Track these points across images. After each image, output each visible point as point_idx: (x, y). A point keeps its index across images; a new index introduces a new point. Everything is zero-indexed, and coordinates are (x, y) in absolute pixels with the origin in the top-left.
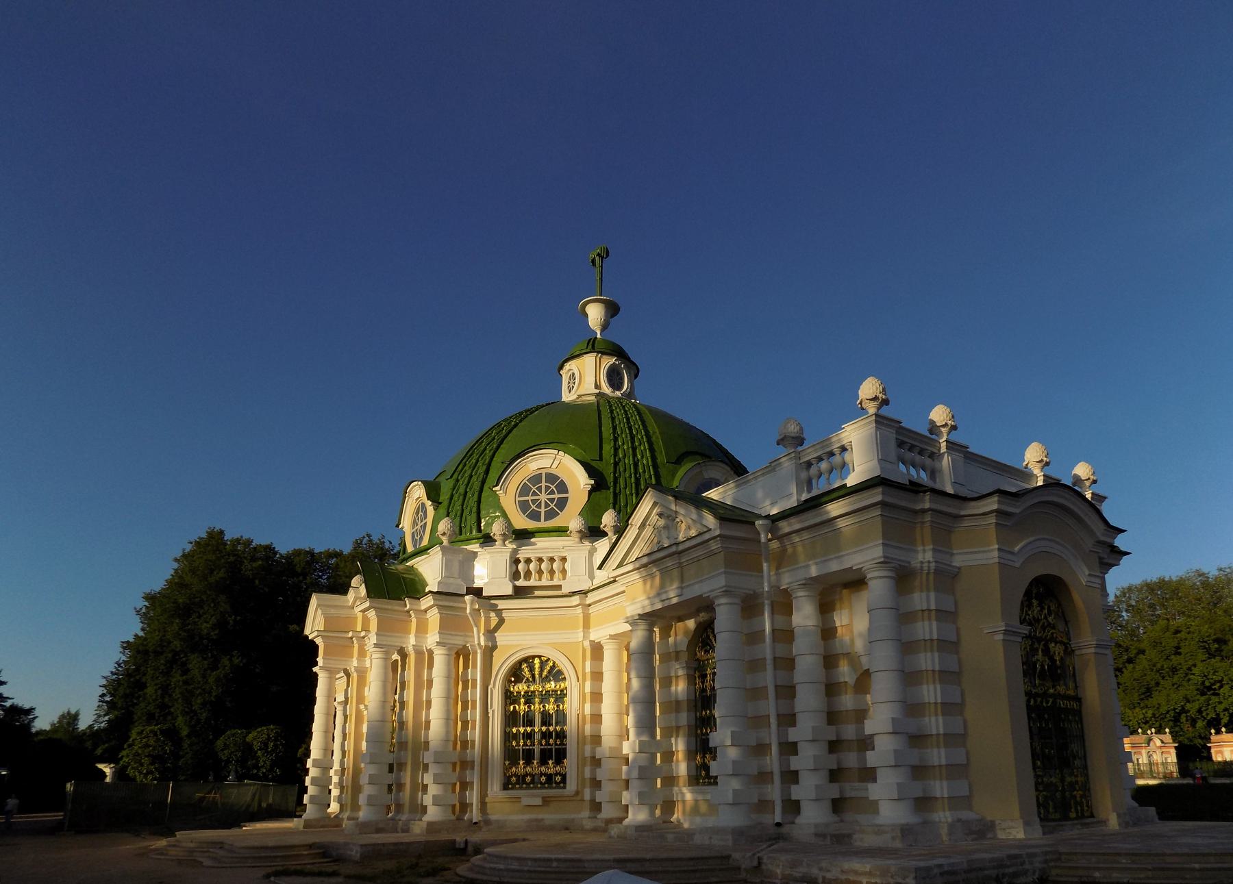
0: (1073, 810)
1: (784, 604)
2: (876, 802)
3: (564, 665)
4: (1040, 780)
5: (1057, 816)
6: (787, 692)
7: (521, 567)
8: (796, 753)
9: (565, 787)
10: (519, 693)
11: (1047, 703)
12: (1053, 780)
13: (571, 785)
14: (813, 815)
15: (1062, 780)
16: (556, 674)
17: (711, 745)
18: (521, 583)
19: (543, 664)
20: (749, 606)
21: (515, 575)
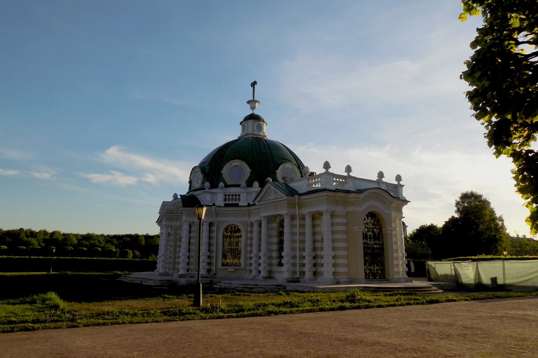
0: (378, 276)
1: (303, 218)
2: (323, 272)
3: (241, 227)
4: (367, 267)
5: (372, 278)
6: (303, 241)
7: (227, 197)
8: (305, 259)
9: (240, 266)
10: (228, 236)
11: (377, 246)
12: (371, 268)
13: (242, 266)
14: (308, 275)
15: (374, 268)
16: (239, 231)
17: (282, 255)
18: (227, 202)
19: (235, 227)
20: (293, 218)
21: (225, 200)
